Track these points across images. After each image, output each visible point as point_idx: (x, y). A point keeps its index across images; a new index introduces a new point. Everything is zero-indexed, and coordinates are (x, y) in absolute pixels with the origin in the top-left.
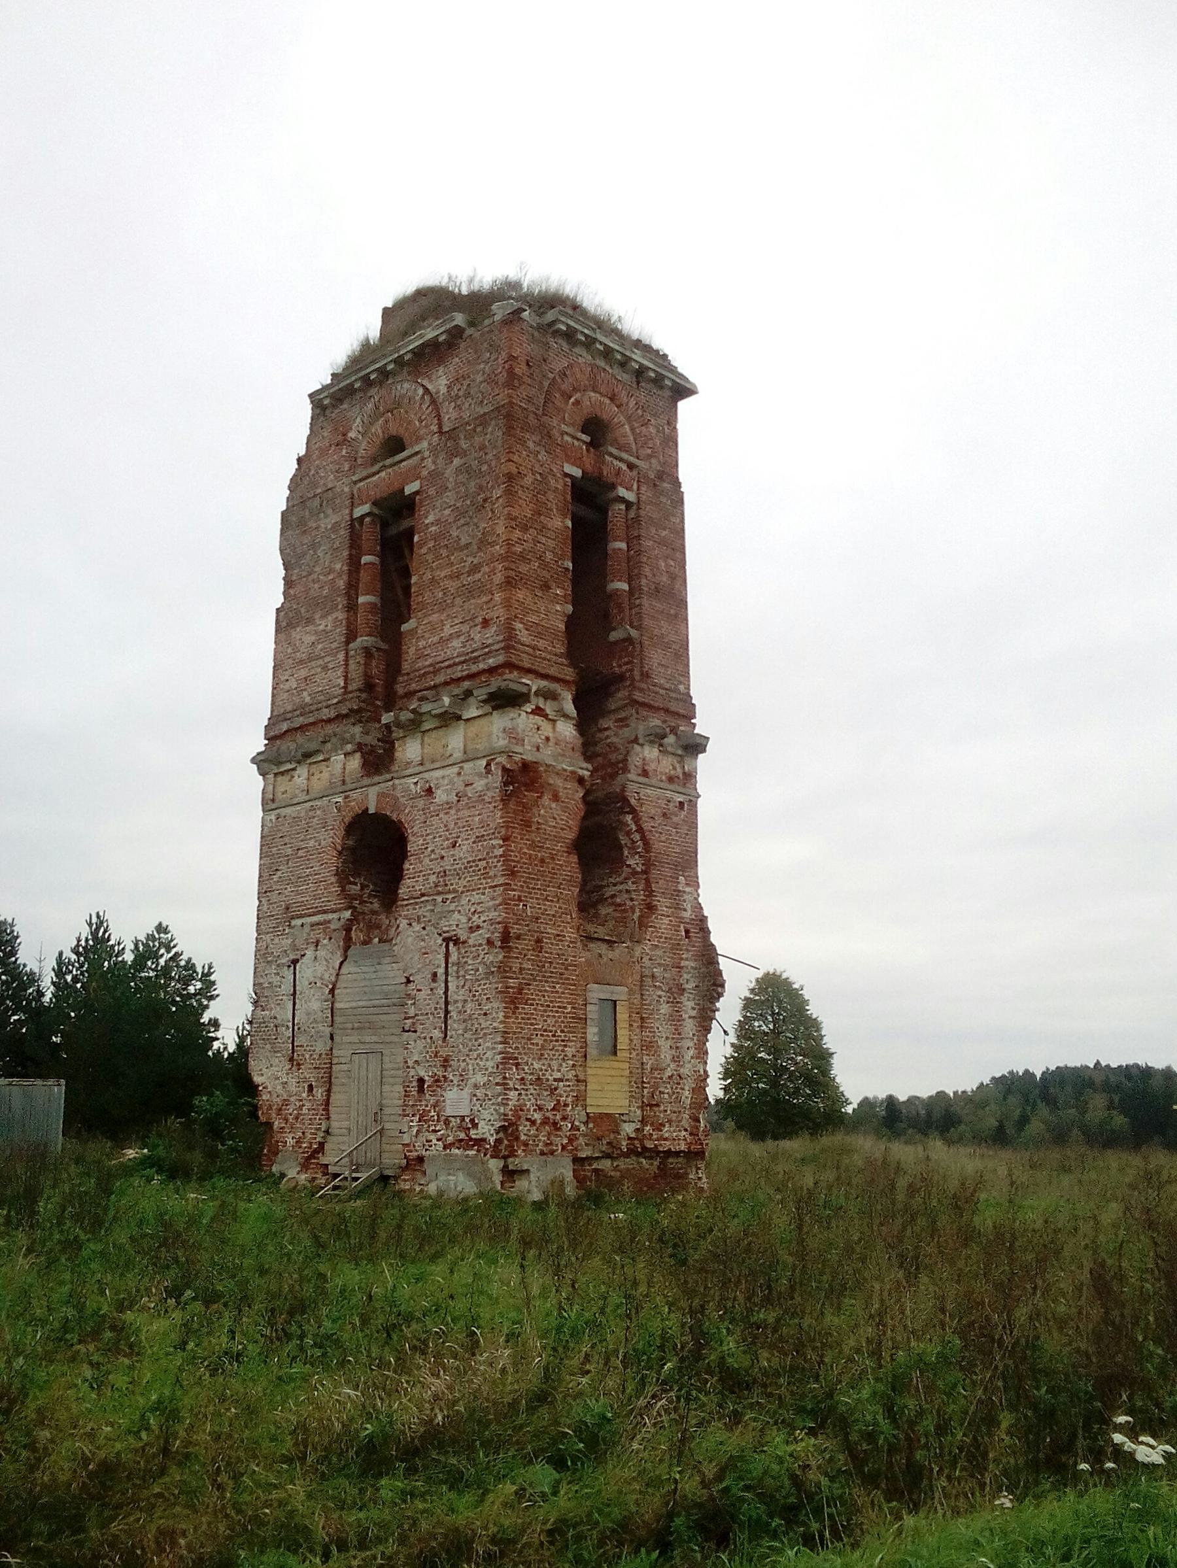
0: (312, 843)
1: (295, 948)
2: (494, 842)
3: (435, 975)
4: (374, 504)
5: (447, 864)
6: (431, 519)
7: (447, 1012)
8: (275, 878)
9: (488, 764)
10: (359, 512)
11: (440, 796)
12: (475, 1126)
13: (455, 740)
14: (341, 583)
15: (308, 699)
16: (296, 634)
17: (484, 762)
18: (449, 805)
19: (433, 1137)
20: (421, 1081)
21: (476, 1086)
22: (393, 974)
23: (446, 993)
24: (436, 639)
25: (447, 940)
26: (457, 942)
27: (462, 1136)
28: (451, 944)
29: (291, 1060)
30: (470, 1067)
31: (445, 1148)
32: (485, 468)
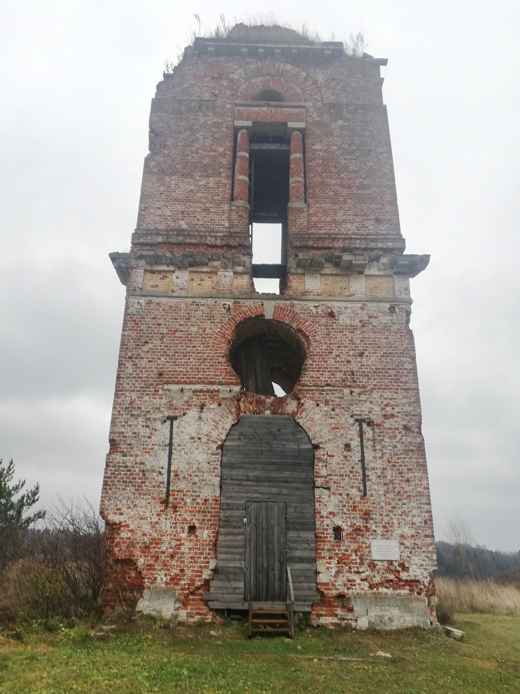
0: (194, 329)
1: (170, 406)
2: (404, 359)
3: (347, 447)
4: (253, 123)
5: (354, 366)
6: (318, 147)
7: (365, 476)
8: (145, 348)
9: (392, 310)
10: (239, 123)
11: (344, 320)
12: (405, 568)
13: (358, 286)
14: (225, 161)
15: (184, 226)
16: (172, 181)
17: (388, 306)
18: (353, 329)
19: (357, 578)
20: (337, 530)
21: (402, 536)
23: (362, 461)
25: (361, 422)
26: (370, 423)
27: (391, 577)
28: (364, 425)
29: (165, 502)
30: (395, 521)
31: (371, 587)
32: (367, 133)
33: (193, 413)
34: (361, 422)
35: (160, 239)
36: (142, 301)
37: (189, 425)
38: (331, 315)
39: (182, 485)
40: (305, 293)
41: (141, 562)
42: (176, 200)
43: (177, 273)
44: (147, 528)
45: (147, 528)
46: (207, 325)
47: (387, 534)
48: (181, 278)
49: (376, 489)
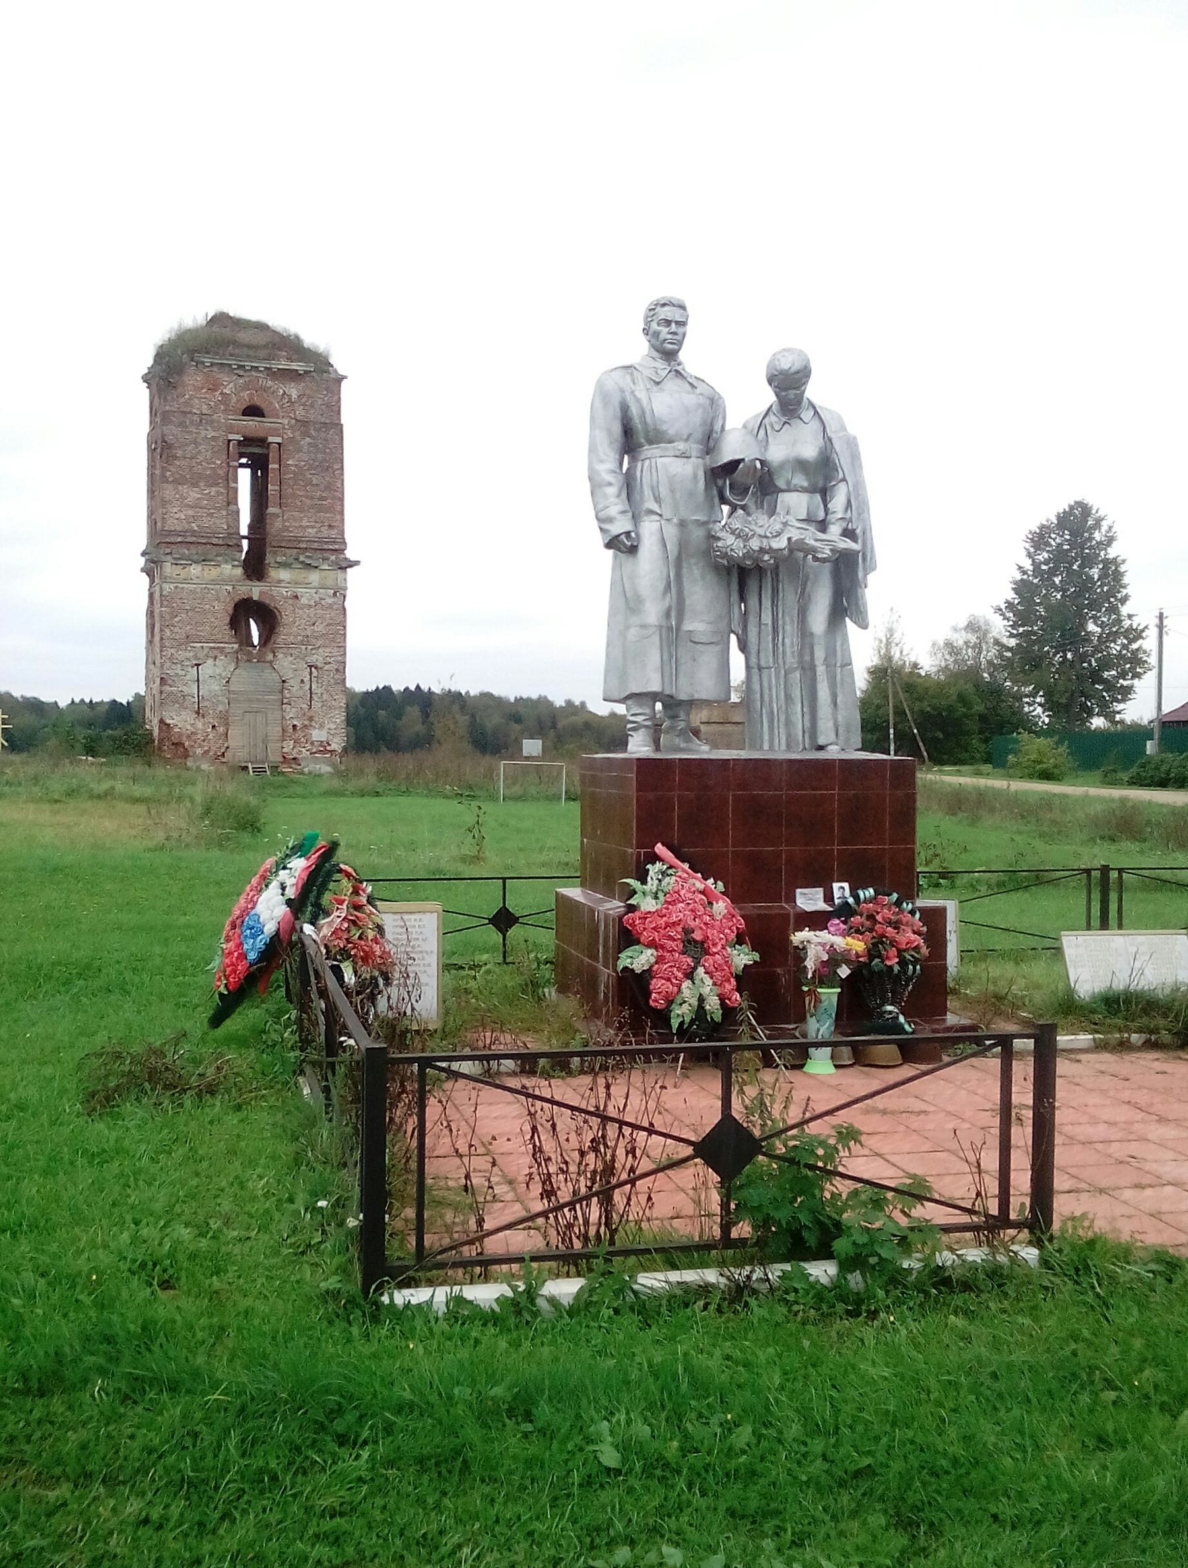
9: (335, 593)
10: (231, 437)
11: (304, 601)
13: (314, 577)
16: (184, 489)
20: (294, 726)
22: (270, 677)
24: (297, 524)
25: (310, 667)
29: (198, 713)
33: (210, 662)
34: (310, 667)
35: (179, 539)
36: (172, 586)
37: (207, 669)
38: (296, 597)
39: (206, 704)
40: (280, 581)
41: (187, 744)
42: (189, 506)
43: (194, 566)
44: (189, 727)
45: (189, 727)
46: (216, 604)
47: (322, 726)
48: (195, 570)
49: (316, 705)
